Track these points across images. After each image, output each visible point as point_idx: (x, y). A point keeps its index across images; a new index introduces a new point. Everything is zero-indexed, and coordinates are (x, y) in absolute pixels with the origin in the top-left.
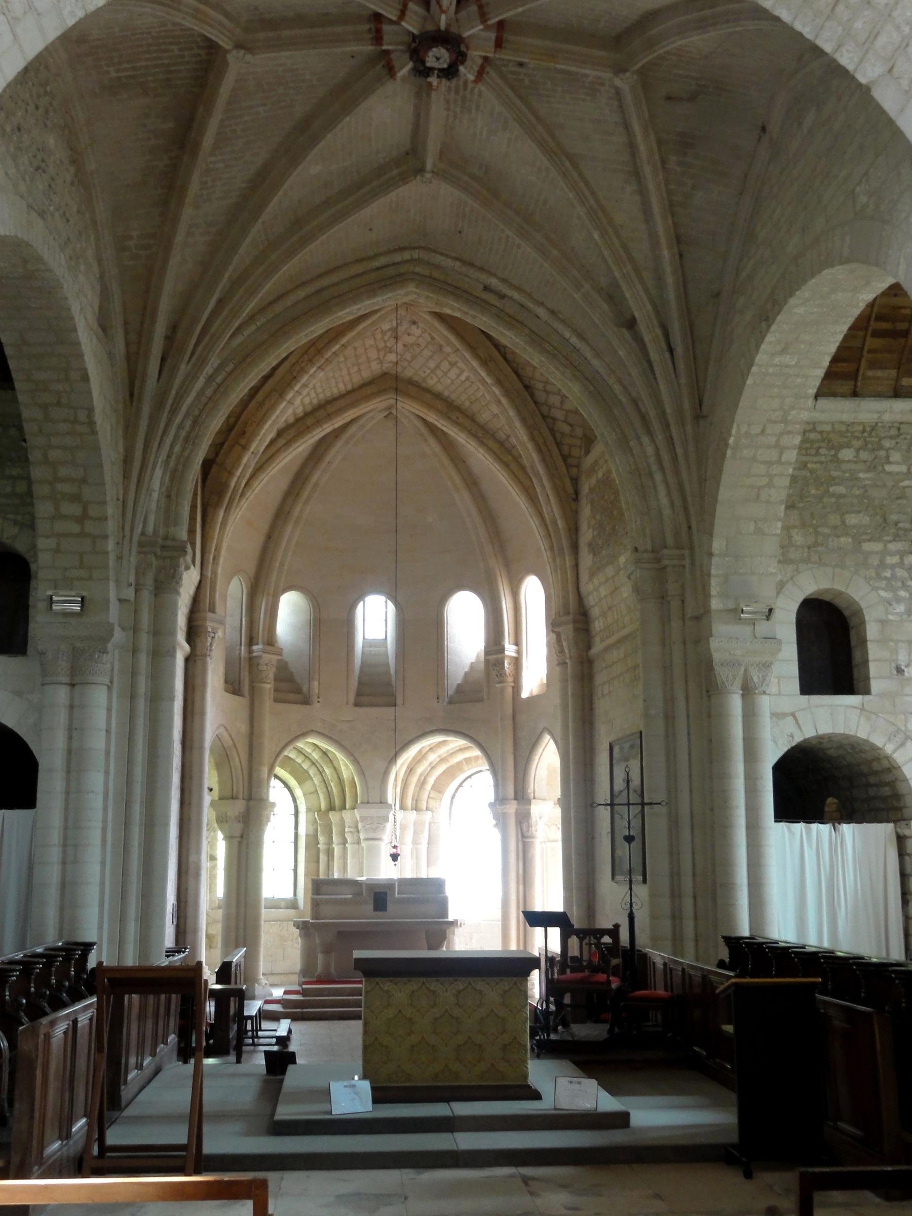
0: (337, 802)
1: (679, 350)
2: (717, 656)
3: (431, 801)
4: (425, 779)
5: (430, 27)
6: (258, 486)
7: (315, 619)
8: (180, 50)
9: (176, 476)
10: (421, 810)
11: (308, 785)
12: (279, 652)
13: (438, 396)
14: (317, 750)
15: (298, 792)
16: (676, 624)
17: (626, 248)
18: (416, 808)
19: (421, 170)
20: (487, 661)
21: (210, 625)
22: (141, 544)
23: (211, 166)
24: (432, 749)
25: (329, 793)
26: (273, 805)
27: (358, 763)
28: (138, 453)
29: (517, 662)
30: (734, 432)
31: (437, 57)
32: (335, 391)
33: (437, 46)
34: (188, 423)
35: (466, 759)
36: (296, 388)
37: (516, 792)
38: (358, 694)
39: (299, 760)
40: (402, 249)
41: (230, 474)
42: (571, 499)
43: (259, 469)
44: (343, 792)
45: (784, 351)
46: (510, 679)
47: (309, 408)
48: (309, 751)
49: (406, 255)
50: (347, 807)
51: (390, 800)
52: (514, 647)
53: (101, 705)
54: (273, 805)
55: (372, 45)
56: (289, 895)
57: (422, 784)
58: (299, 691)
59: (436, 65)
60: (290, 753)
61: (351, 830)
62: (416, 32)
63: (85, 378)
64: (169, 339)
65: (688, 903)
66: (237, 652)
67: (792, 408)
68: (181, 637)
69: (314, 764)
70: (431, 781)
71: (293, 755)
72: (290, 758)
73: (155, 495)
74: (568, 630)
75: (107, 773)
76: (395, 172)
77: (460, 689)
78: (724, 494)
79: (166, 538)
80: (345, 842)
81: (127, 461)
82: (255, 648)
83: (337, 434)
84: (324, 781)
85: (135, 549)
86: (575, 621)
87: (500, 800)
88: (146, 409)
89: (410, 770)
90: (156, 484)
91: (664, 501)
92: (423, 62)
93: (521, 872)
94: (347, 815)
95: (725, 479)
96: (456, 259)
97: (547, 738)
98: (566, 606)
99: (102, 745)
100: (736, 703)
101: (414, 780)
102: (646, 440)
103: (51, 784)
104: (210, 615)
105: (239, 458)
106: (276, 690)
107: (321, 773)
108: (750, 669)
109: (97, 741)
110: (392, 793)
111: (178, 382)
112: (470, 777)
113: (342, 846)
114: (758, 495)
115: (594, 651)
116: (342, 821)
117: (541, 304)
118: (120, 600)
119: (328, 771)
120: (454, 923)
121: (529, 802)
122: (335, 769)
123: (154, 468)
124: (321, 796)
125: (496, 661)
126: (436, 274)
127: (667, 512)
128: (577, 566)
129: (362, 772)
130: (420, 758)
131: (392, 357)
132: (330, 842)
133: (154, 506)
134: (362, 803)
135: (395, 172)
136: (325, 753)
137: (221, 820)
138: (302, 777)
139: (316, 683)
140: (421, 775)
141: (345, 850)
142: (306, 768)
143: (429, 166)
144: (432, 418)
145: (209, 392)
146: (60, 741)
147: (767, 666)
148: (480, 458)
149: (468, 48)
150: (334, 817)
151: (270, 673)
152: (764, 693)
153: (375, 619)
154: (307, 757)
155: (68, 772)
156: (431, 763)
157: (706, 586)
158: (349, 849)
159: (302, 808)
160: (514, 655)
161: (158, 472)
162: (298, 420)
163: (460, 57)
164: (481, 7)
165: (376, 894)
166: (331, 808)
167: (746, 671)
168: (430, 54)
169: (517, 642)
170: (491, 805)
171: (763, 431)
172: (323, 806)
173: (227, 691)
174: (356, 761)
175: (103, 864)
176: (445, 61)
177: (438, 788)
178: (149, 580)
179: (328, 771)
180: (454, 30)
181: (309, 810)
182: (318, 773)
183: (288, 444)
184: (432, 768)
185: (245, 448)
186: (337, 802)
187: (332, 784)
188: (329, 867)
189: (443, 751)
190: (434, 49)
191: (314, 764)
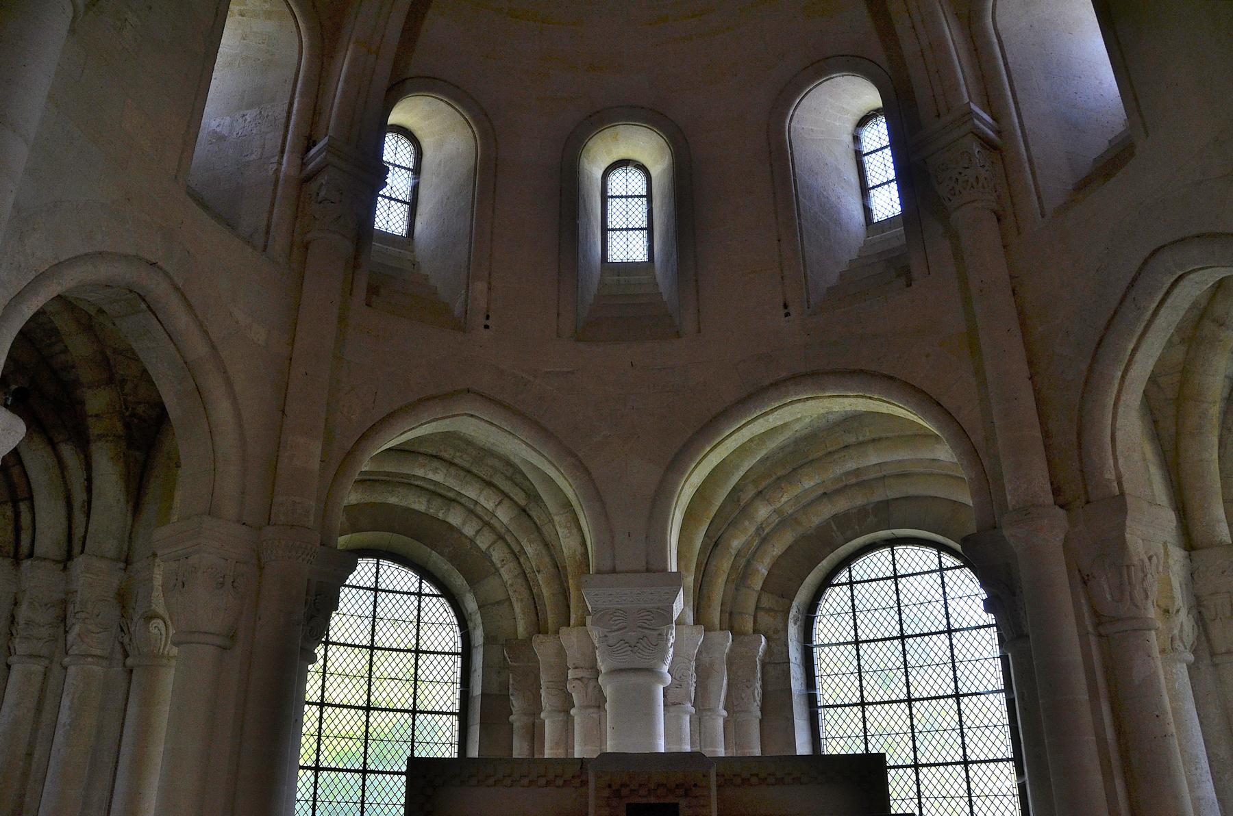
0: (551, 619)
4: (748, 563)
10: (744, 634)
14: (506, 502)
15: (471, 605)
27: (588, 472)
35: (835, 517)
37: (1056, 491)
39: (469, 530)
48: (490, 505)
50: (572, 622)
57: (741, 576)
61: (580, 674)
66: (275, 166)
69: (501, 538)
71: (455, 518)
72: (451, 527)
89: (714, 545)
93: (1110, 734)
94: (570, 639)
101: (724, 565)
107: (517, 555)
113: (561, 717)
116: (561, 652)
122: (546, 545)
124: (518, 608)
132: (535, 709)
134: (598, 572)
139: (480, 286)
141: (568, 722)
142: (483, 547)
156: (760, 528)
158: (577, 720)
159: (478, 637)
166: (539, 627)
174: (580, 468)
177: (781, 587)
181: (489, 640)
182: (509, 556)
184: (764, 540)
187: (539, 577)
191: (501, 538)
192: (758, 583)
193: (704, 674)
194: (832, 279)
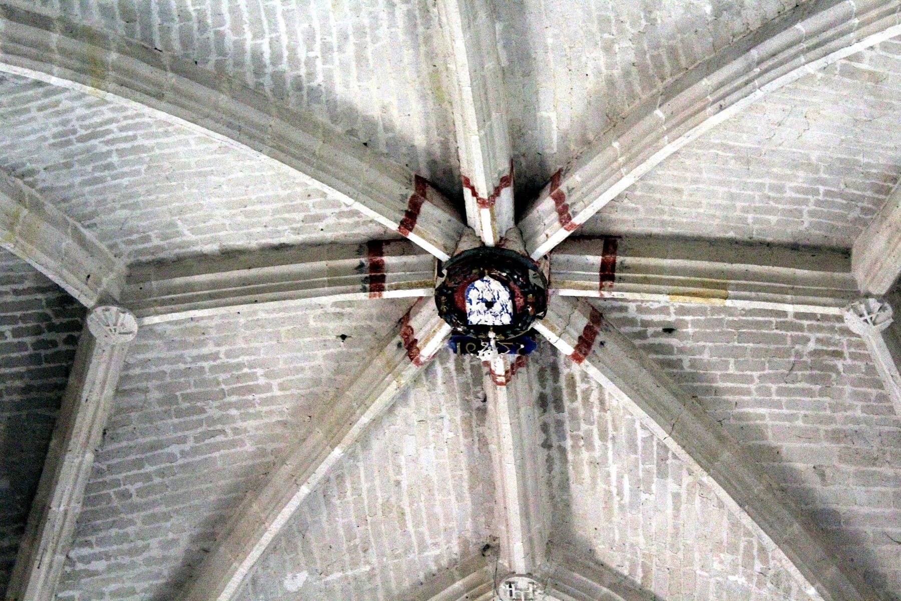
5: (466, 245)
8: (16, 333)
23: (80, 566)
31: (489, 301)
33: (481, 277)
55: (364, 290)
59: (488, 319)
62: (444, 257)
76: (458, 585)
92: (463, 316)
135: (458, 585)
149: (547, 284)
163: (532, 299)
164: (559, 199)
168: (473, 294)
176: (504, 307)
180: (515, 246)
190: (478, 284)
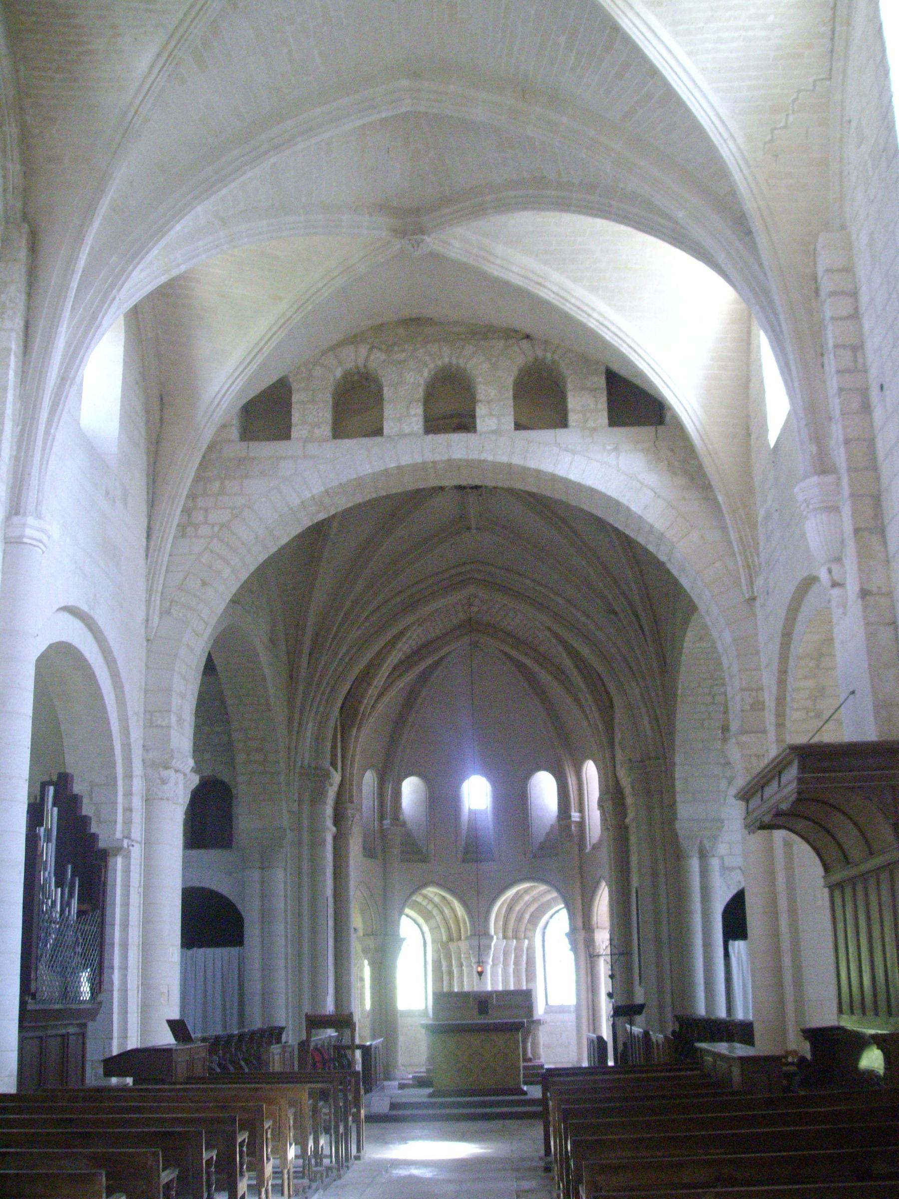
0: (455, 935)
1: (646, 629)
2: (681, 833)
3: (529, 934)
6: (380, 707)
7: (430, 798)
9: (321, 725)
11: (432, 922)
12: (404, 824)
13: (510, 635)
16: (657, 811)
17: (606, 568)
18: (516, 937)
19: (469, 529)
20: (560, 826)
21: (350, 812)
22: (301, 774)
24: (526, 891)
25: (449, 929)
26: (404, 939)
28: (297, 718)
29: (581, 825)
30: (680, 686)
32: (433, 635)
34: (329, 689)
36: (404, 640)
38: (466, 851)
39: (425, 903)
40: (464, 564)
41: (360, 702)
42: (606, 707)
43: (381, 694)
44: (459, 926)
45: (701, 639)
46: (576, 839)
47: (415, 648)
48: (432, 896)
49: (468, 567)
50: (463, 937)
51: (492, 932)
52: (578, 814)
53: (280, 878)
54: (404, 939)
56: (423, 1007)
57: (520, 919)
58: (419, 852)
60: (414, 898)
63: (264, 679)
64: (314, 641)
65: (668, 999)
67: (715, 670)
68: (329, 822)
70: (527, 916)
73: (308, 741)
74: (609, 805)
75: (286, 923)
77: (542, 847)
78: (679, 725)
79: (316, 768)
80: (461, 965)
81: (290, 720)
82: (385, 822)
83: (437, 664)
84: (445, 919)
85: (297, 775)
86: (612, 799)
87: (573, 930)
88: (301, 688)
89: (510, 909)
90: (309, 734)
91: (648, 727)
95: (679, 716)
96: (501, 568)
97: (603, 884)
98: (607, 787)
99: (282, 905)
100: (694, 864)
101: (513, 917)
102: (634, 684)
103: (252, 932)
104: (349, 805)
105: (366, 691)
106: (402, 852)
107: (442, 912)
108: (705, 841)
109: (280, 904)
110: (493, 925)
111: (321, 665)
112: (557, 911)
114: (703, 725)
115: (627, 820)
116: (459, 948)
117: (560, 595)
118: (289, 812)
119: (446, 911)
120: (534, 1022)
121: (593, 931)
123: (307, 723)
125: (567, 827)
126: (489, 579)
127: (649, 733)
128: (613, 757)
129: (469, 911)
130: (517, 898)
131: (475, 609)
132: (450, 965)
133: (308, 748)
136: (444, 898)
137: (366, 951)
138: (427, 916)
140: (519, 911)
141: (462, 971)
143: (473, 526)
144: (507, 649)
145: (340, 669)
146: (257, 902)
147: (714, 838)
148: (545, 677)
150: (453, 946)
151: (398, 840)
152: (714, 856)
153: (477, 794)
154: (431, 901)
155: (263, 922)
157: (673, 786)
160: (578, 819)
161: (310, 725)
162: (408, 657)
165: (480, 1003)
166: (451, 939)
167: (701, 842)
169: (581, 810)
170: (567, 935)
171: (699, 686)
172: (444, 938)
173: (364, 856)
175: (287, 981)
178: (307, 796)
179: (447, 911)
181: (433, 941)
183: (400, 675)
185: (369, 684)
186: (455, 935)
188: (450, 984)
189: (534, 893)
192: (526, 921)
193: (506, 954)
194: (541, 838)
